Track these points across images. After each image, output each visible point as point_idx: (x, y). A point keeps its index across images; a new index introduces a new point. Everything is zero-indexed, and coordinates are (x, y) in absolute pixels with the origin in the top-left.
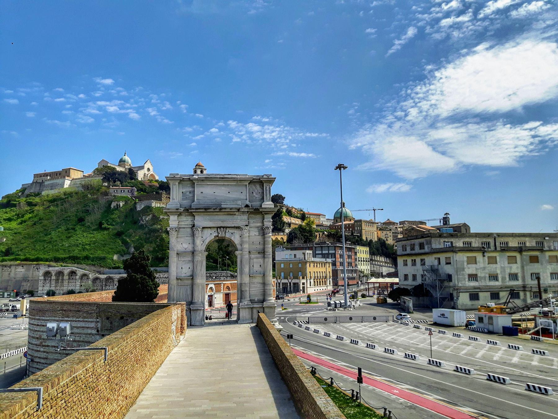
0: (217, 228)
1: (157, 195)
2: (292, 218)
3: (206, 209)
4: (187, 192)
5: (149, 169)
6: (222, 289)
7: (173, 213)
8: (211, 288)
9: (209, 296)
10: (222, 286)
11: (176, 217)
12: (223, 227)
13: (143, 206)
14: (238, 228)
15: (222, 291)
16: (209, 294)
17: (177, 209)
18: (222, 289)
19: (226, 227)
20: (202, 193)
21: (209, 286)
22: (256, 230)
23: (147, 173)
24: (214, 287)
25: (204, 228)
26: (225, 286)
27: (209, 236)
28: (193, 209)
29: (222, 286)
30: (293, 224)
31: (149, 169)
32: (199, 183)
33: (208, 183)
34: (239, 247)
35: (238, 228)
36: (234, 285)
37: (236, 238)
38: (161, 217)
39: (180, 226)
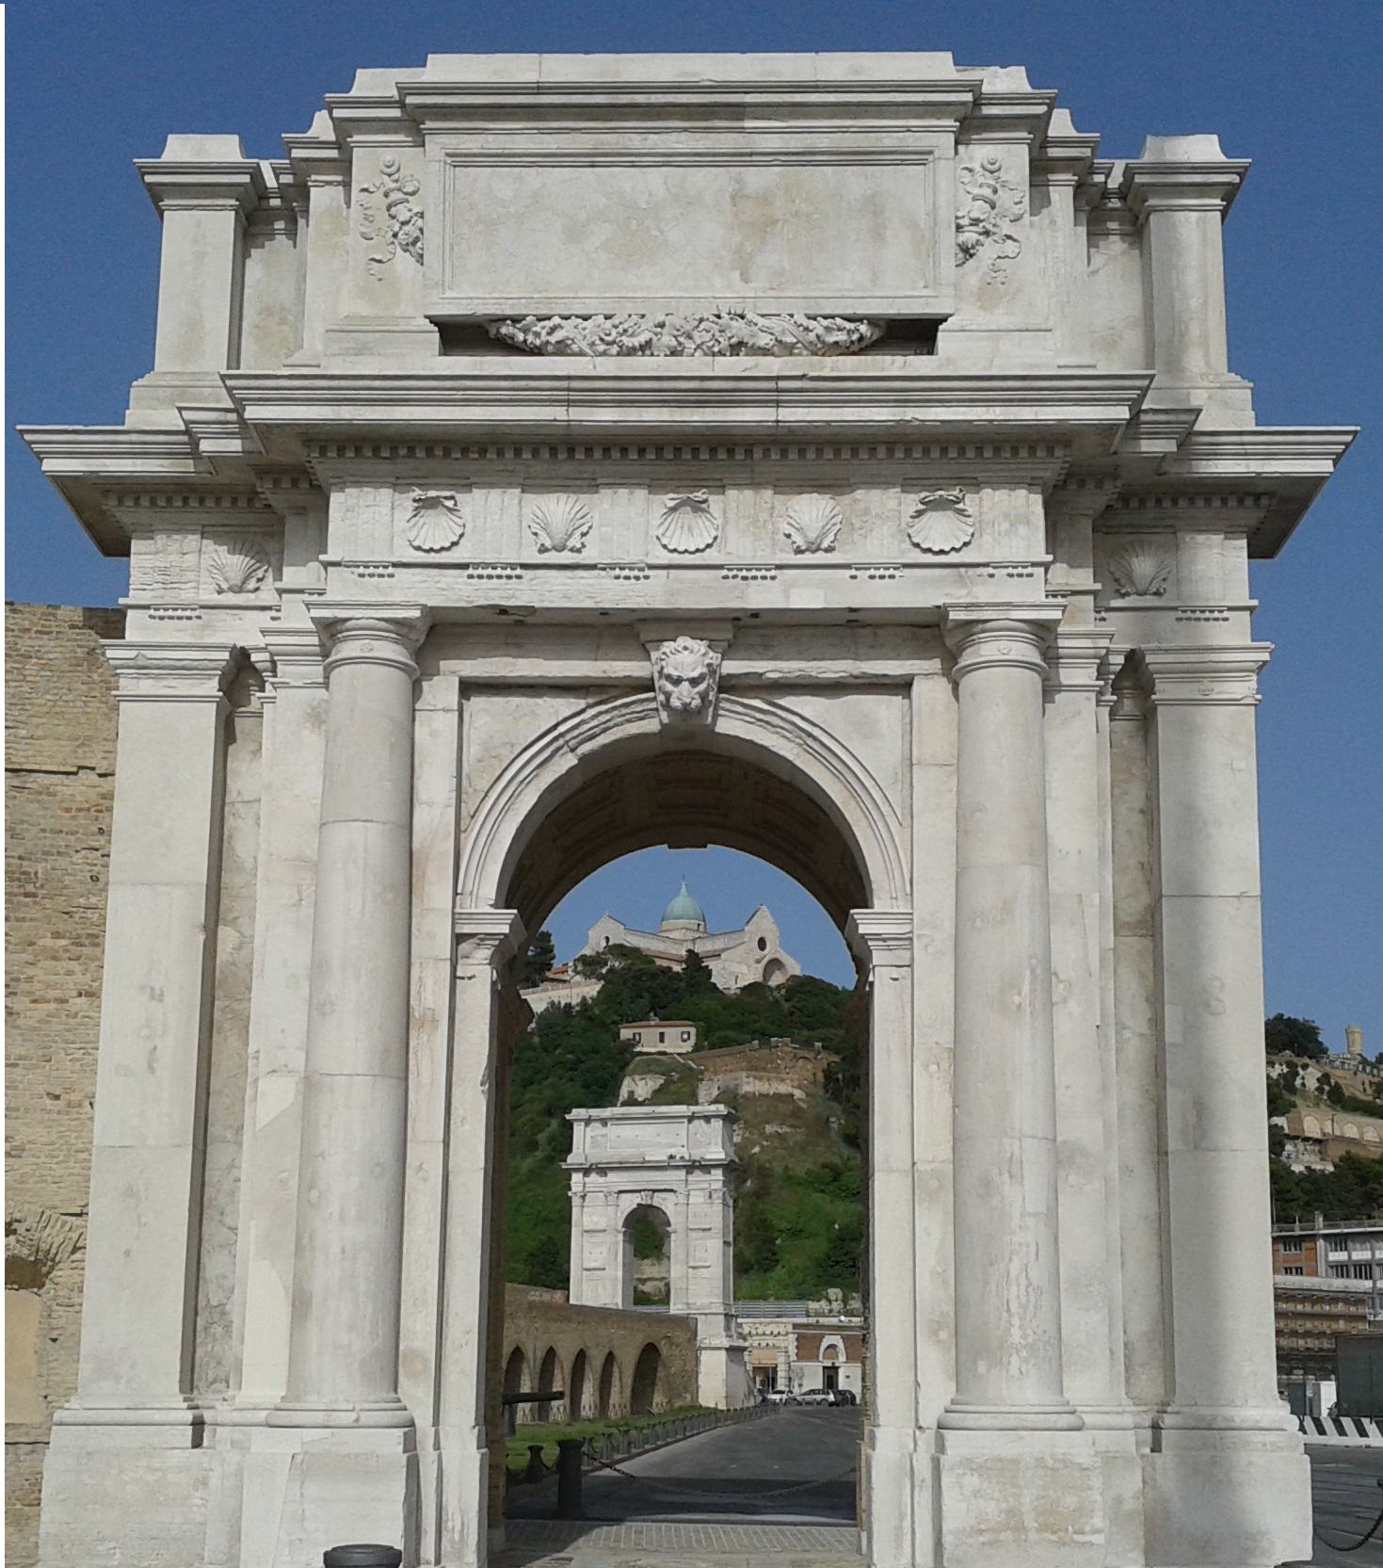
0: (639, 1191)
1: (766, 1051)
2: (1341, 1116)
4: (597, 1135)
5: (762, 944)
7: (577, 1170)
8: (832, 1347)
11: (581, 1175)
13: (716, 1093)
14: (672, 1191)
19: (654, 1191)
21: (824, 1344)
22: (700, 1193)
23: (759, 954)
25: (620, 1192)
27: (630, 1203)
30: (1342, 1139)
31: (762, 944)
37: (668, 1204)
38: (769, 1129)
39: (587, 1189)
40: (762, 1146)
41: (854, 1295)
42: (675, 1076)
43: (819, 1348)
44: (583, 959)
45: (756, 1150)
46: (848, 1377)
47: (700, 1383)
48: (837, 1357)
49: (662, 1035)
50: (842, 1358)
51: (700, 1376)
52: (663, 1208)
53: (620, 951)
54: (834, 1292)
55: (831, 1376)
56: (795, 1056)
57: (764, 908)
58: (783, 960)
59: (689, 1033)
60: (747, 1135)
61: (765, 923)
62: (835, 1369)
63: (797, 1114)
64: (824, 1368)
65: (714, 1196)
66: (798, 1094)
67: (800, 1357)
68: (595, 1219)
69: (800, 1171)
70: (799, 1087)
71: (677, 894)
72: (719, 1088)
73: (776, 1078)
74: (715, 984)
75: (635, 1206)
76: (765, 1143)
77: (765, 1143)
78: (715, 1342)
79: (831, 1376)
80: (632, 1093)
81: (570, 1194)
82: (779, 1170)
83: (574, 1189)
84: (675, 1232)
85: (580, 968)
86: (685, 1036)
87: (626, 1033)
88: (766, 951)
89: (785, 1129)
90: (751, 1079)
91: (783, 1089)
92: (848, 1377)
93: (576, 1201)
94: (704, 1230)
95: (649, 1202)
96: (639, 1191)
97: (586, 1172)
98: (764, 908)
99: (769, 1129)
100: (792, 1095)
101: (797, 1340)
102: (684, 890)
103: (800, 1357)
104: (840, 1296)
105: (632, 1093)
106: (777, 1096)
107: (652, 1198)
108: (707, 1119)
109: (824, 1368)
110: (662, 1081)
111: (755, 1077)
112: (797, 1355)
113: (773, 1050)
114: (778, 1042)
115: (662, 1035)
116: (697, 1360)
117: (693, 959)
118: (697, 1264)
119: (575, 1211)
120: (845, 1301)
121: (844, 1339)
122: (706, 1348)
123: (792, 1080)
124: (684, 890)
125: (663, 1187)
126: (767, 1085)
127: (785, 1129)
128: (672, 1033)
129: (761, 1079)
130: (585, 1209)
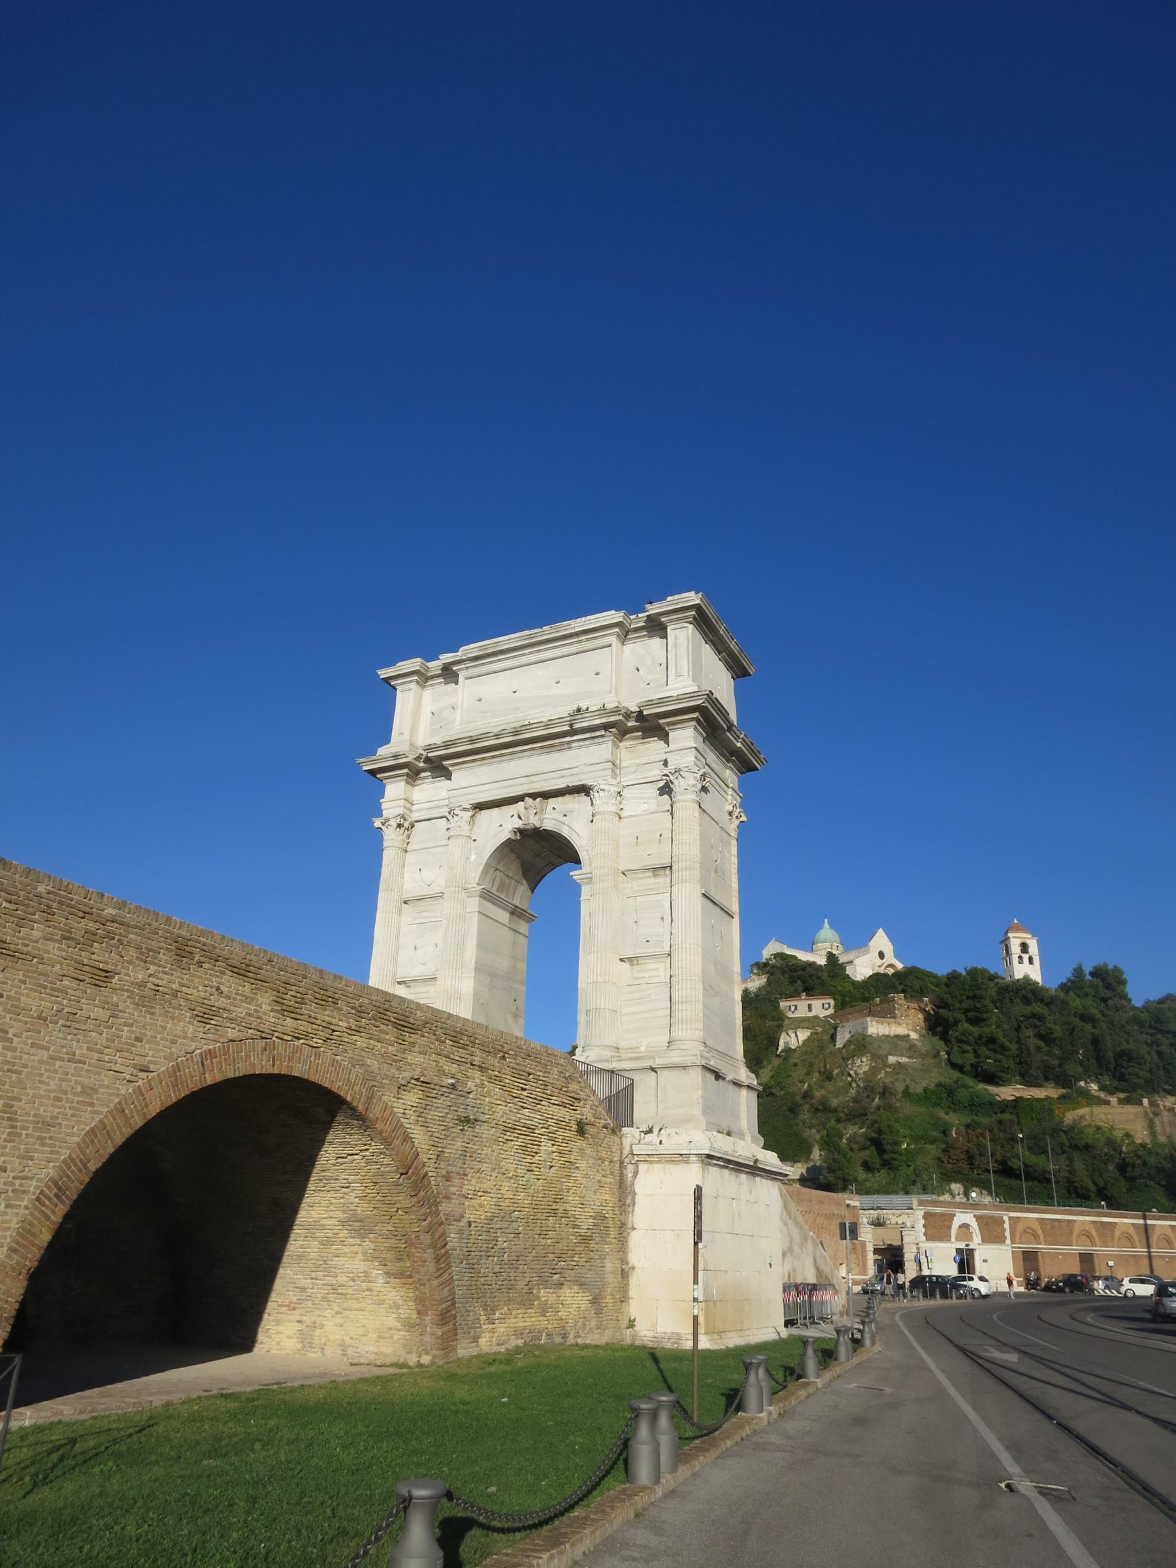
1: (886, 1005)
3: (472, 740)
5: (881, 955)
6: (1007, 1234)
8: (965, 1226)
9: (959, 1251)
10: (1007, 1226)
12: (534, 796)
13: (848, 1036)
14: (584, 790)
15: (1008, 1241)
16: (962, 1245)
17: (396, 756)
18: (1007, 1234)
20: (480, 700)
23: (879, 961)
24: (974, 1225)
26: (1020, 1228)
28: (437, 748)
29: (1007, 1226)
31: (881, 955)
32: (471, 672)
33: (496, 666)
34: (583, 856)
35: (584, 790)
36: (1053, 1227)
38: (892, 1059)
39: (415, 816)
40: (886, 1072)
41: (974, 1189)
42: (819, 1029)
43: (949, 1227)
44: (757, 965)
45: (881, 1075)
46: (985, 1261)
47: (633, 1258)
48: (972, 1240)
49: (810, 1007)
50: (977, 1238)
51: (636, 1240)
52: (565, 832)
53: (780, 956)
54: (956, 1187)
55: (965, 1261)
56: (908, 1008)
57: (881, 931)
58: (894, 964)
59: (829, 1004)
60: (874, 1064)
61: (881, 941)
62: (971, 1252)
63: (912, 1049)
64: (958, 1250)
65: (678, 785)
66: (914, 1036)
67: (929, 1237)
68: (428, 875)
69: (919, 1089)
70: (915, 1031)
71: (821, 926)
72: (850, 1032)
73: (895, 1023)
74: (848, 975)
75: (506, 834)
76: (888, 1069)
77: (888, 1069)
78: (674, 1141)
79: (965, 1261)
80: (787, 1043)
81: (377, 823)
82: (900, 1087)
83: (385, 813)
84: (590, 880)
85: (755, 971)
86: (826, 1006)
87: (783, 1004)
88: (884, 961)
89: (904, 1060)
90: (874, 1023)
91: (901, 1030)
92: (985, 1261)
93: (391, 837)
94: (656, 870)
95: (538, 825)
96: (520, 798)
97: (413, 773)
98: (881, 931)
99: (892, 1059)
100: (908, 1035)
101: (924, 1217)
102: (826, 925)
103: (929, 1237)
104: (962, 1190)
105: (787, 1043)
106: (897, 1036)
107: (543, 811)
108: (656, 627)
109: (958, 1250)
110: (809, 1034)
111: (877, 1021)
112: (925, 1234)
113: (891, 1003)
114: (894, 997)
115: (810, 1007)
116: (624, 1193)
117: (831, 957)
118: (639, 952)
119: (389, 857)
120: (966, 1194)
121: (978, 1218)
122: (652, 1158)
123: (907, 1025)
124: (826, 925)
125: (561, 784)
126: (887, 1028)
127: (904, 1060)
128: (817, 1004)
129: (882, 1023)
130: (410, 857)
